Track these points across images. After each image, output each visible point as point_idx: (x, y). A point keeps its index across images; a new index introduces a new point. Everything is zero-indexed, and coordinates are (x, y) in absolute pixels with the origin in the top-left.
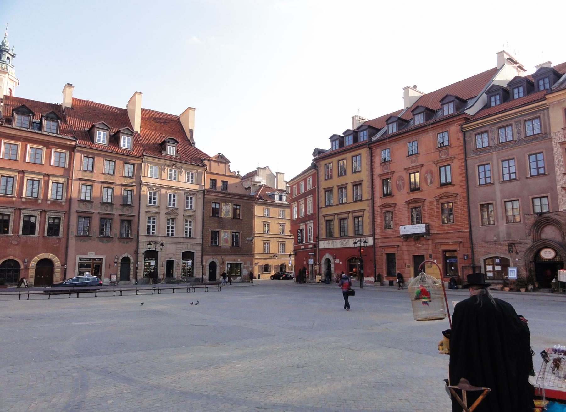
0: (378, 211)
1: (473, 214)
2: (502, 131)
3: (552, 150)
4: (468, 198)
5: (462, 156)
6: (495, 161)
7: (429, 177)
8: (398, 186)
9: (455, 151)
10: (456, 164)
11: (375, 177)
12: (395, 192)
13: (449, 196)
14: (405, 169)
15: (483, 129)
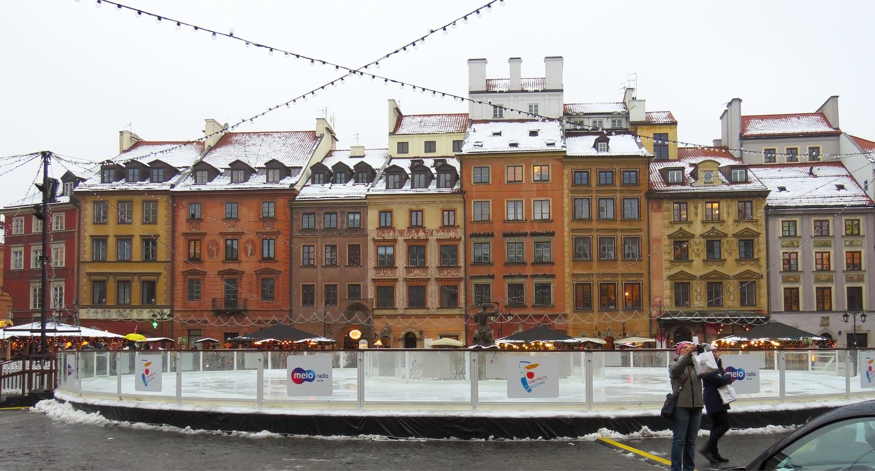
0: (180, 280)
1: (295, 293)
2: (328, 217)
3: (367, 246)
4: (291, 276)
5: (288, 233)
6: (319, 245)
7: (250, 248)
8: (209, 251)
9: (279, 226)
10: (281, 240)
11: (178, 235)
12: (206, 257)
13: (272, 272)
14: (221, 233)
15: (310, 211)
